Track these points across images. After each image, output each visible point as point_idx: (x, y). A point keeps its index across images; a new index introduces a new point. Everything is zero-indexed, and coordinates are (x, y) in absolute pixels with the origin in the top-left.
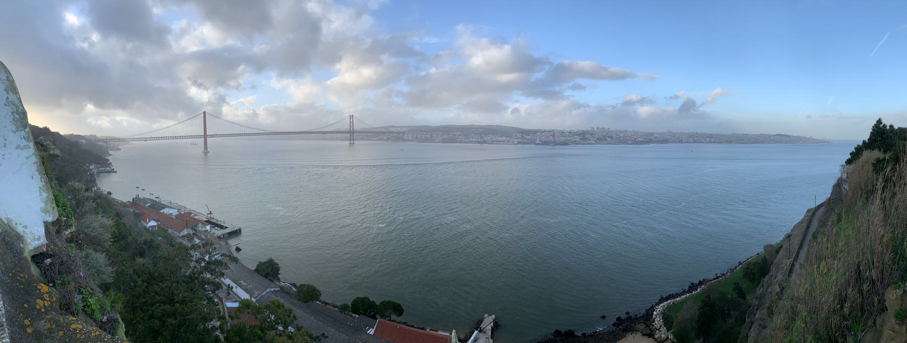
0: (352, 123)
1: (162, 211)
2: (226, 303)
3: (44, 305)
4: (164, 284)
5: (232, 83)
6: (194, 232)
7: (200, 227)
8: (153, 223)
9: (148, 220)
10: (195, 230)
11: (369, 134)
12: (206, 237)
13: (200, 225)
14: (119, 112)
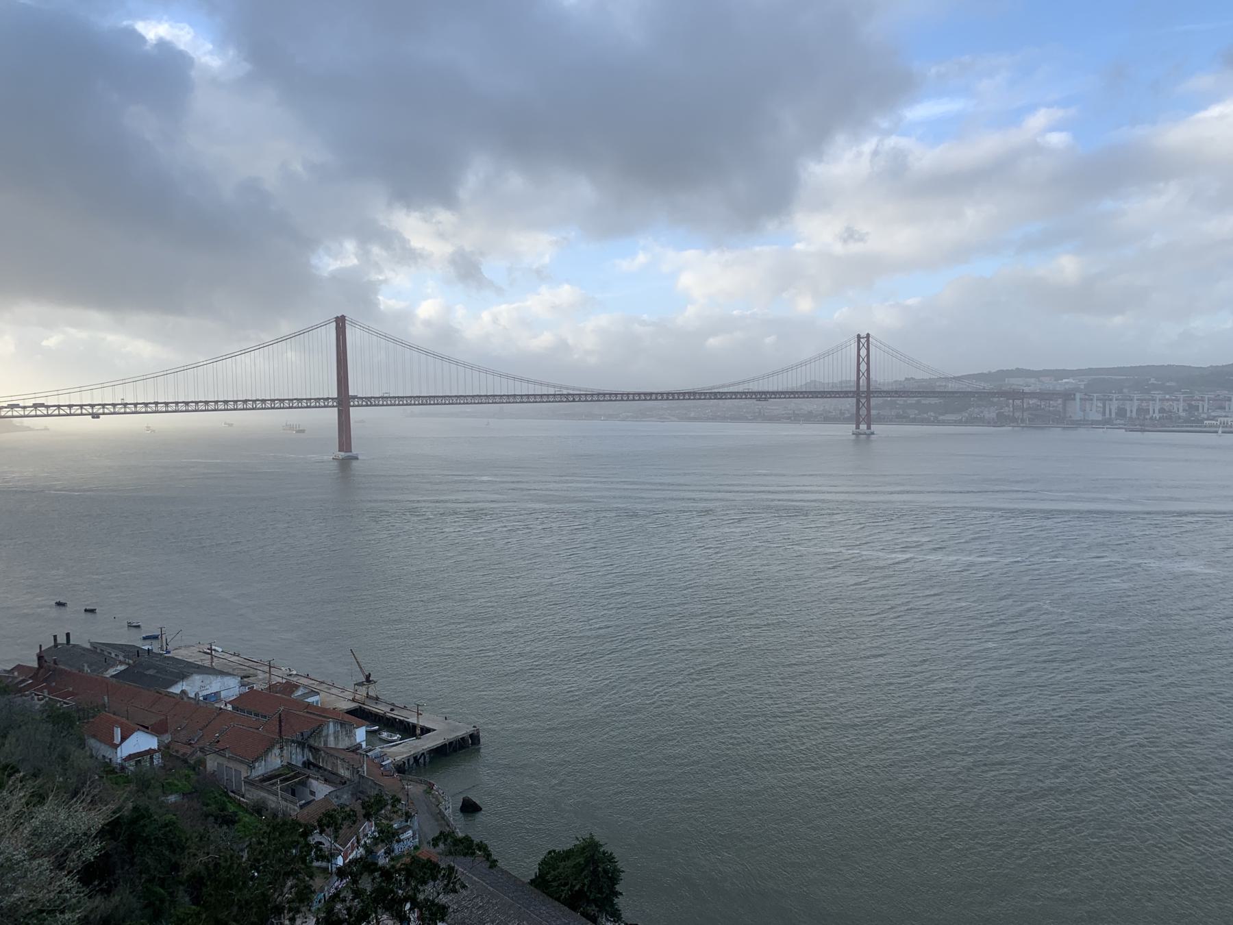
0: (863, 361)
1: (176, 689)
7: (332, 737)
8: (143, 742)
9: (118, 732)
10: (311, 748)
11: (925, 401)
12: (355, 771)
13: (331, 724)
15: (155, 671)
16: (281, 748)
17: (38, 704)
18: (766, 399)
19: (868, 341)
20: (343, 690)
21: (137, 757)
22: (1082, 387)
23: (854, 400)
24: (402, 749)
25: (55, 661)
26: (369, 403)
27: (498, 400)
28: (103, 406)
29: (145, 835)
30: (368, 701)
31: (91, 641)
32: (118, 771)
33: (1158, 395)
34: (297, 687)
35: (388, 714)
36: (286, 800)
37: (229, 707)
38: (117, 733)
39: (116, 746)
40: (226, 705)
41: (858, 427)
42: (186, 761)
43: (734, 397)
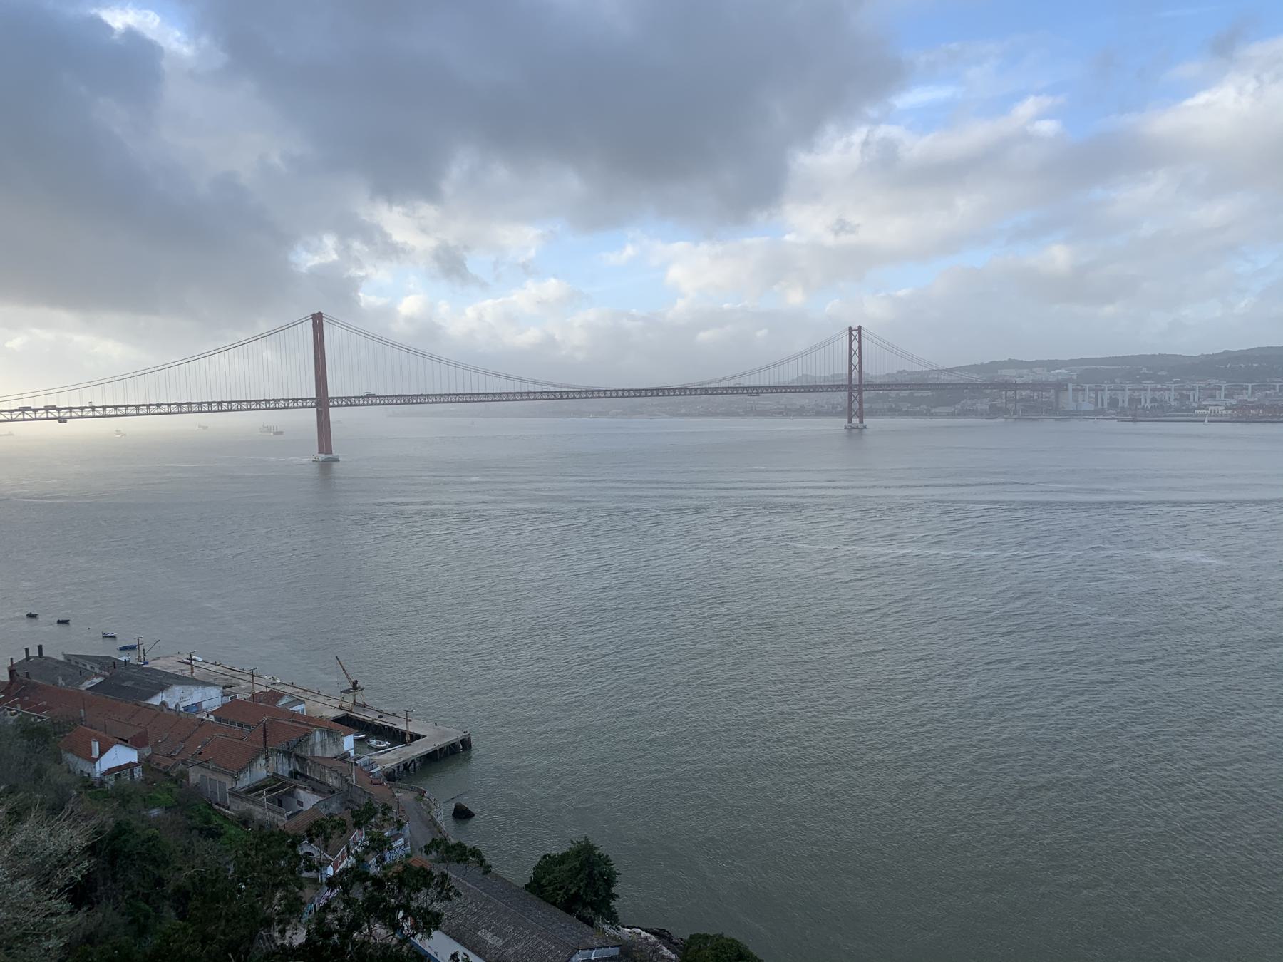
1: (155, 701)
6: (295, 765)
7: (319, 746)
8: (121, 755)
9: (96, 746)
10: (297, 757)
11: (918, 394)
12: (343, 779)
13: (318, 733)
15: (133, 682)
16: (267, 759)
17: (11, 719)
18: (757, 394)
19: (860, 333)
20: (330, 698)
21: (117, 771)
22: (1075, 377)
23: (847, 393)
24: (392, 757)
25: (27, 674)
26: (349, 403)
27: (483, 398)
28: (70, 409)
29: (126, 850)
30: (355, 709)
31: (65, 653)
32: (97, 786)
33: (1149, 384)
34: (281, 696)
35: (375, 721)
36: (273, 811)
37: (212, 718)
38: (95, 748)
39: (94, 761)
40: (208, 716)
41: (850, 421)
42: (167, 774)
43: (725, 392)
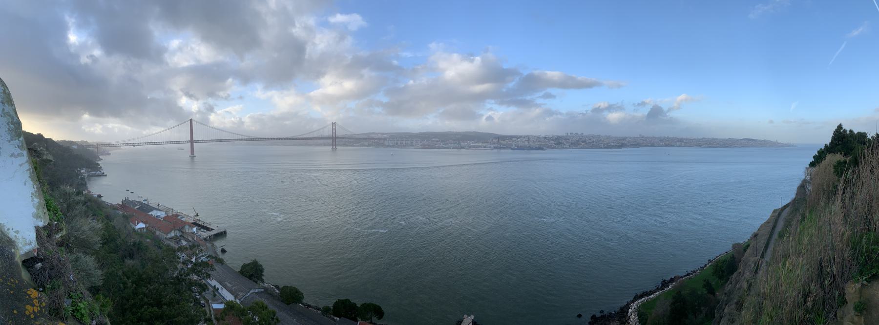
1: (150, 213)
2: (213, 305)
3: (33, 311)
4: (151, 286)
5: (221, 94)
6: (181, 234)
7: (187, 229)
8: (141, 225)
9: (136, 222)
10: (182, 232)
11: (350, 140)
14: (111, 119)
34: (178, 216)
